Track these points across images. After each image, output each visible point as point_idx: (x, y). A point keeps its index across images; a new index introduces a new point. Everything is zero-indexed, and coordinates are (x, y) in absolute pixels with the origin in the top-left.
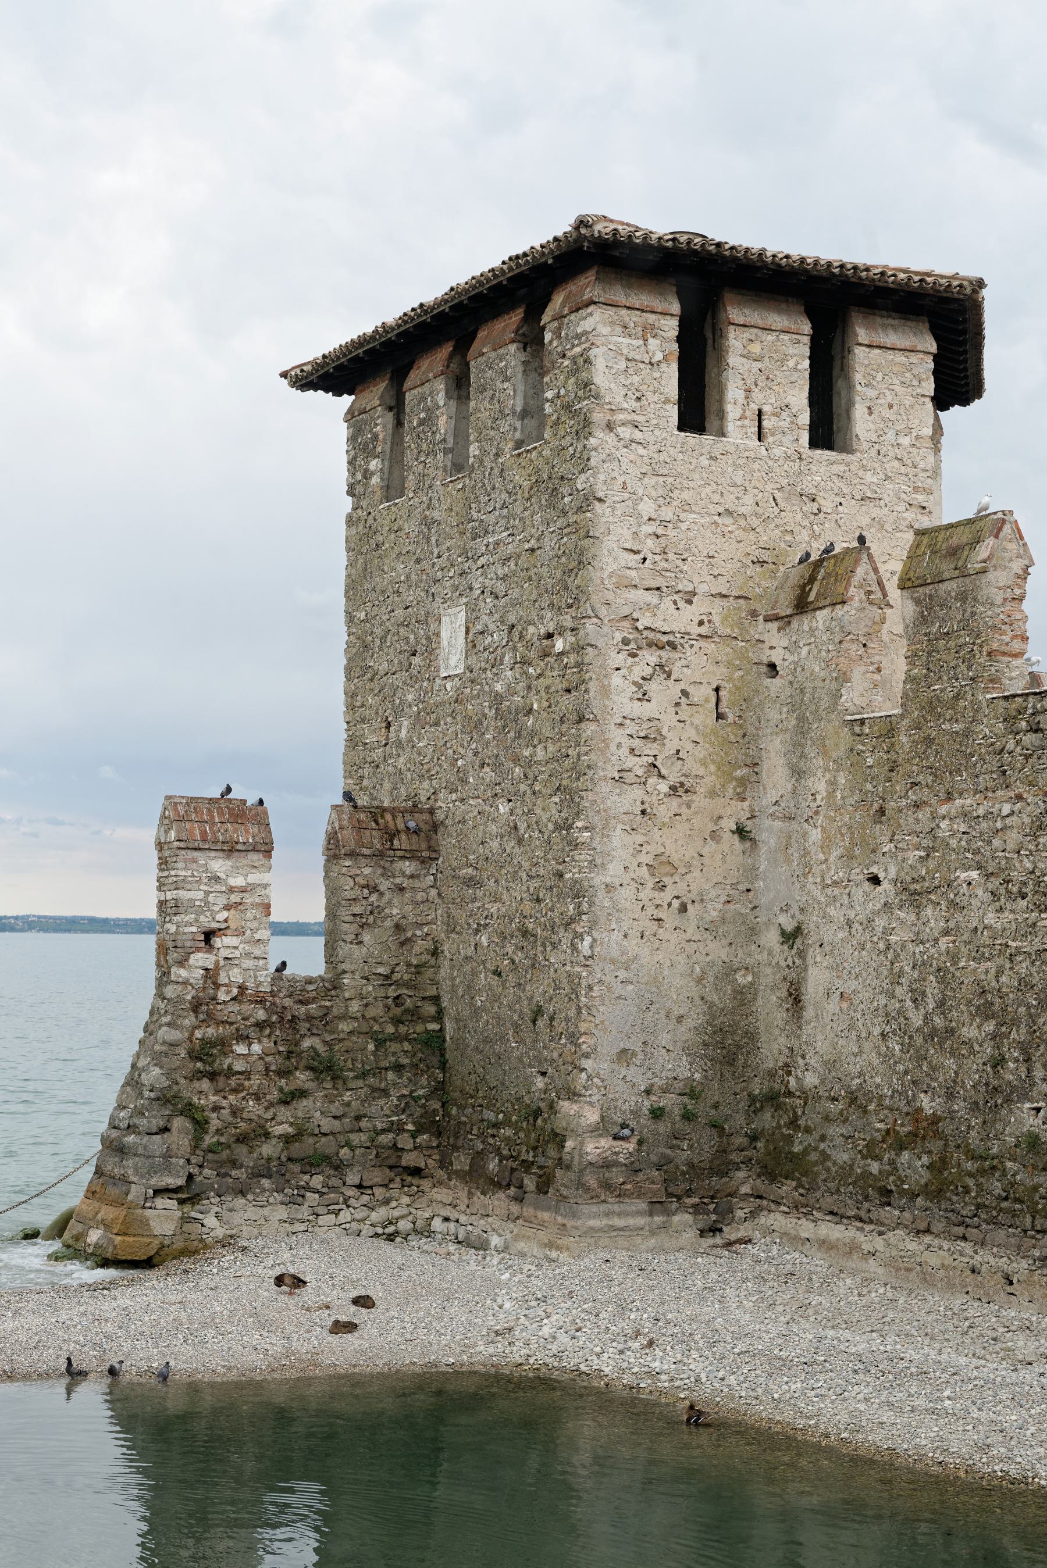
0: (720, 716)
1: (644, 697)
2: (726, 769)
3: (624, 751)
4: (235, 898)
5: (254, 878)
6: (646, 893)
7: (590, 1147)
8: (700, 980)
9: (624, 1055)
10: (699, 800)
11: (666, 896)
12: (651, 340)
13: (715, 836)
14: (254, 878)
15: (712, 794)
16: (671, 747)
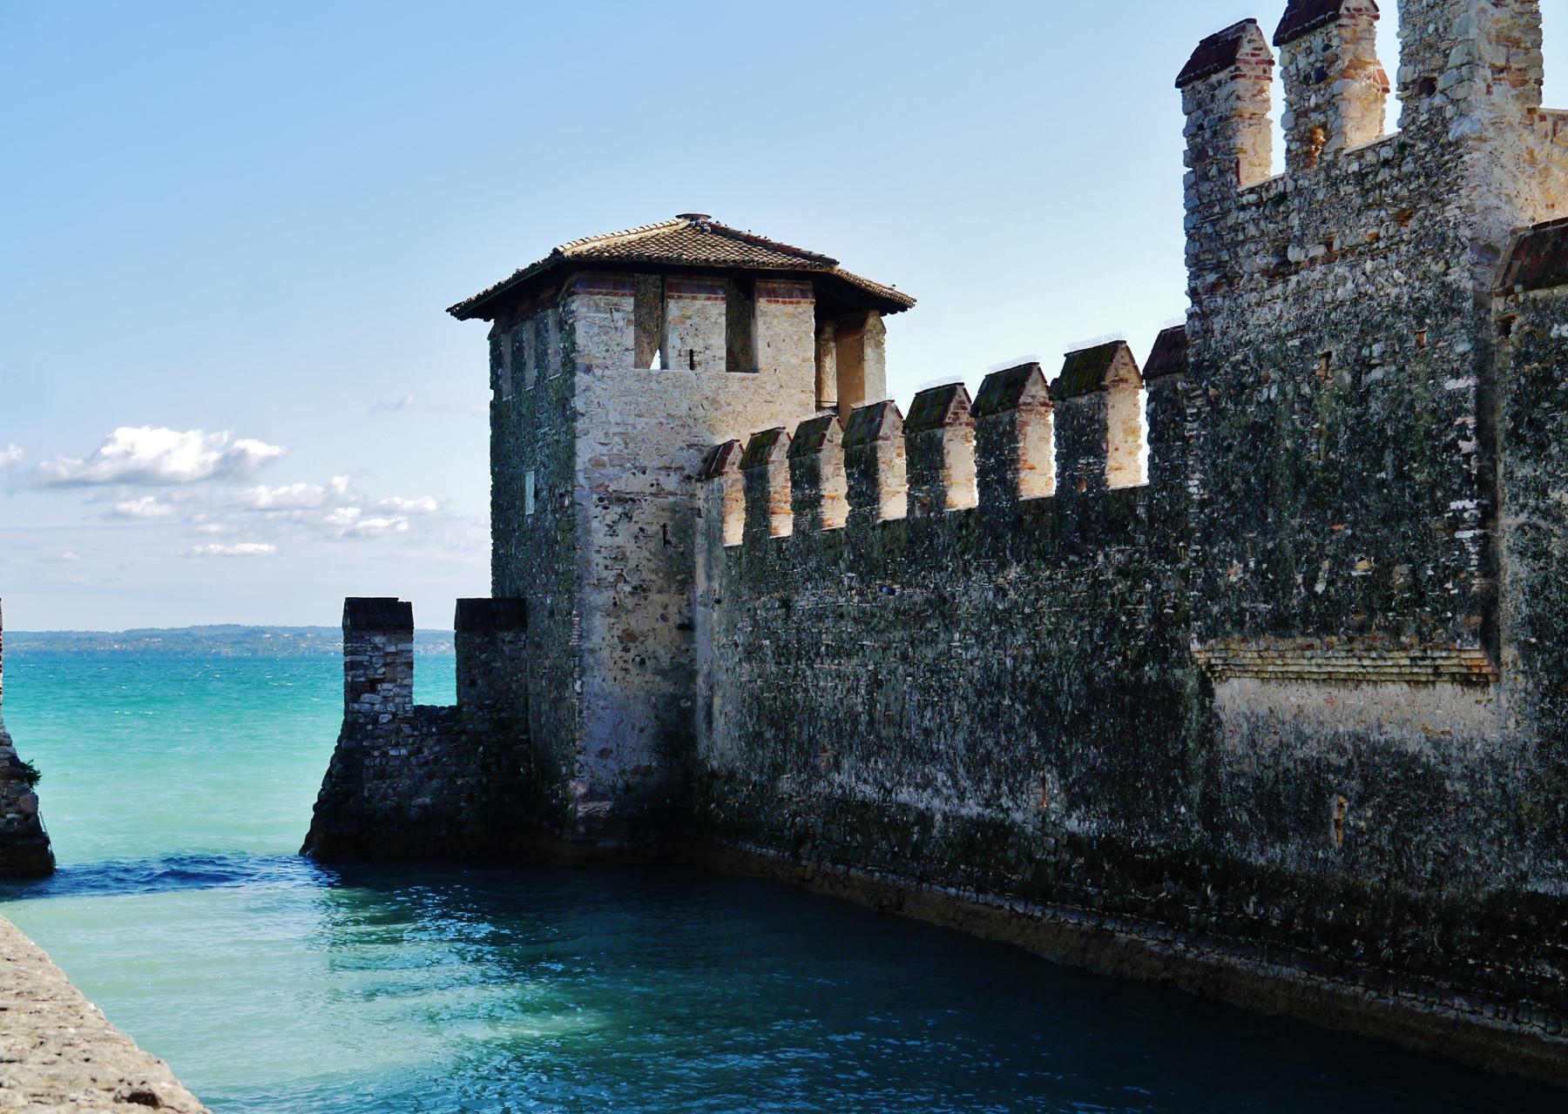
0: (667, 542)
1: (614, 534)
2: (670, 575)
3: (601, 567)
4: (389, 660)
5: (401, 647)
6: (618, 653)
7: (582, 810)
8: (655, 706)
9: (604, 753)
10: (654, 597)
11: (633, 653)
12: (617, 315)
13: (664, 618)
14: (401, 647)
15: (660, 592)
16: (632, 564)
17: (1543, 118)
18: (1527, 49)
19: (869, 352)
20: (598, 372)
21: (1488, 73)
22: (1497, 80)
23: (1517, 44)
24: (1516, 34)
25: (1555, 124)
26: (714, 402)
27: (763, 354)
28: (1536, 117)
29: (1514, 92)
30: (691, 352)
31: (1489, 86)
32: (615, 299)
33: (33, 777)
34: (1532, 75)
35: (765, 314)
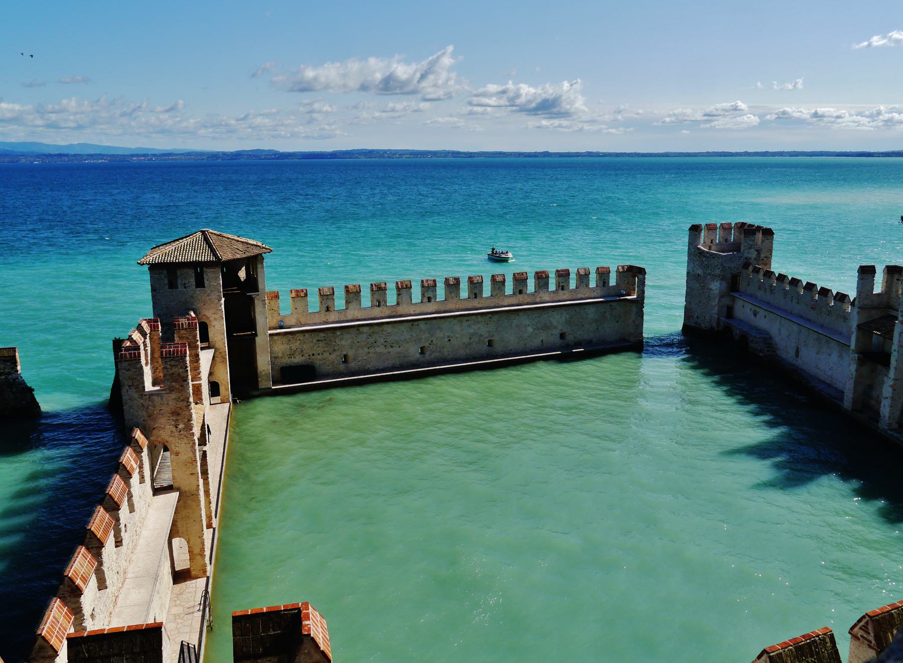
12: (162, 275)
17: (146, 395)
18: (139, 380)
19: (259, 266)
20: (158, 291)
21: (127, 388)
22: (130, 389)
23: (135, 378)
24: (135, 377)
25: (149, 396)
26: (193, 297)
27: (206, 283)
28: (143, 395)
29: (135, 391)
30: (185, 284)
31: (127, 391)
32: (161, 271)
33: (33, 390)
34: (141, 386)
35: (206, 272)
